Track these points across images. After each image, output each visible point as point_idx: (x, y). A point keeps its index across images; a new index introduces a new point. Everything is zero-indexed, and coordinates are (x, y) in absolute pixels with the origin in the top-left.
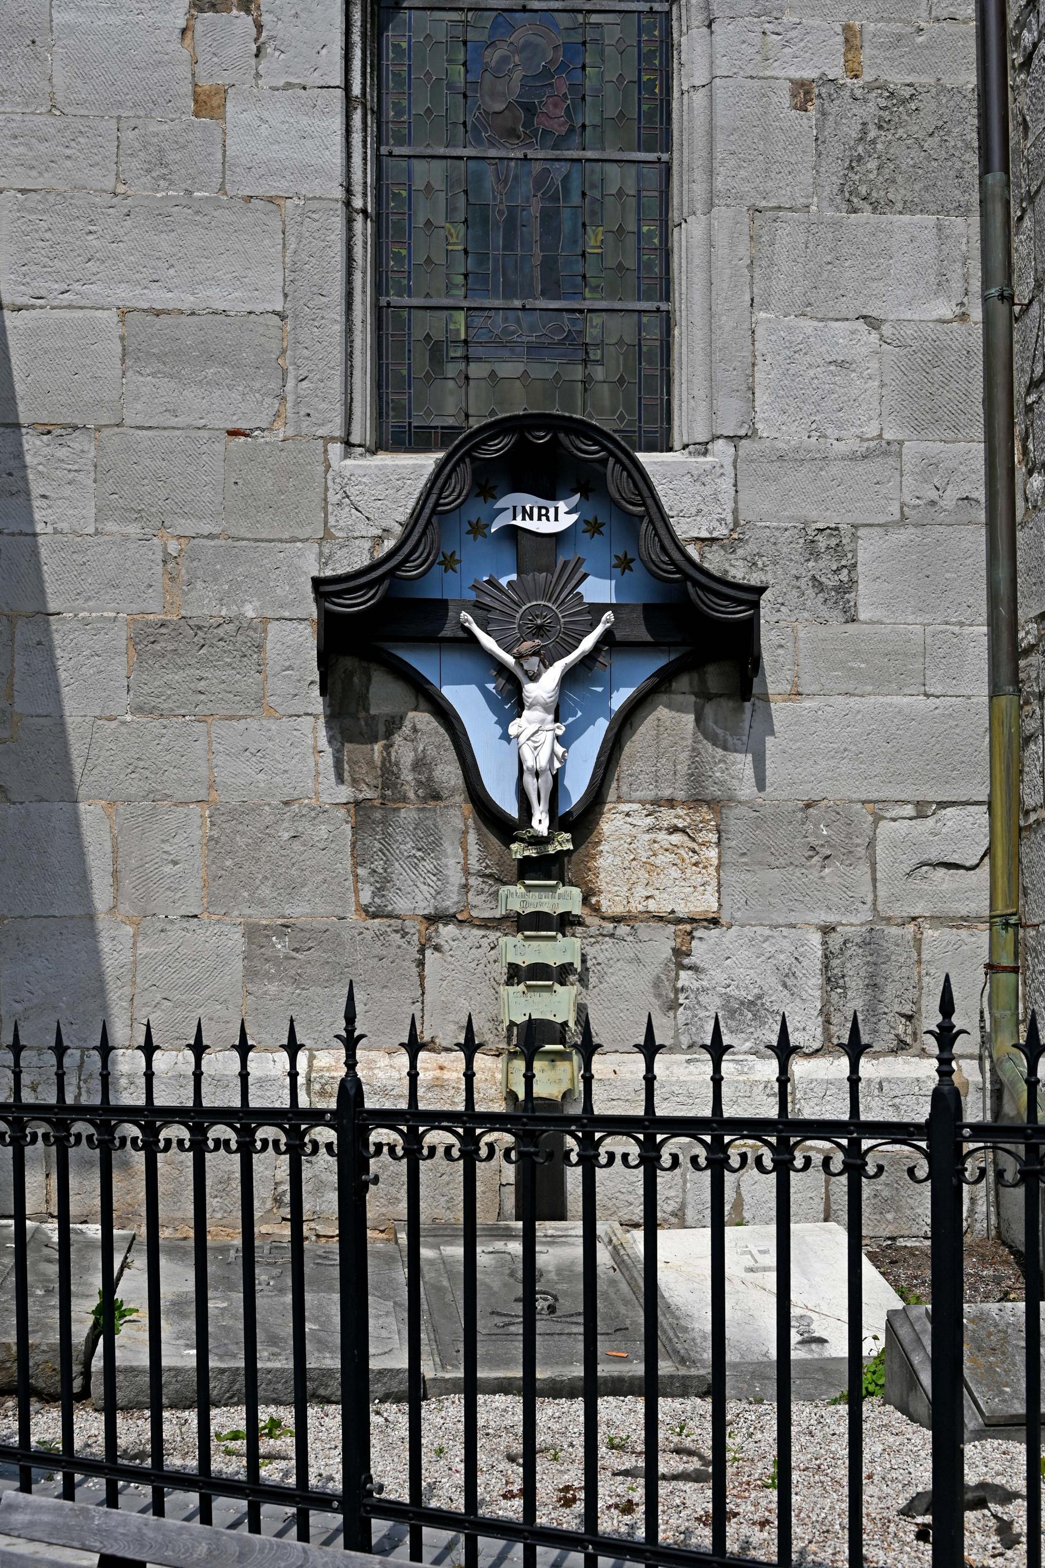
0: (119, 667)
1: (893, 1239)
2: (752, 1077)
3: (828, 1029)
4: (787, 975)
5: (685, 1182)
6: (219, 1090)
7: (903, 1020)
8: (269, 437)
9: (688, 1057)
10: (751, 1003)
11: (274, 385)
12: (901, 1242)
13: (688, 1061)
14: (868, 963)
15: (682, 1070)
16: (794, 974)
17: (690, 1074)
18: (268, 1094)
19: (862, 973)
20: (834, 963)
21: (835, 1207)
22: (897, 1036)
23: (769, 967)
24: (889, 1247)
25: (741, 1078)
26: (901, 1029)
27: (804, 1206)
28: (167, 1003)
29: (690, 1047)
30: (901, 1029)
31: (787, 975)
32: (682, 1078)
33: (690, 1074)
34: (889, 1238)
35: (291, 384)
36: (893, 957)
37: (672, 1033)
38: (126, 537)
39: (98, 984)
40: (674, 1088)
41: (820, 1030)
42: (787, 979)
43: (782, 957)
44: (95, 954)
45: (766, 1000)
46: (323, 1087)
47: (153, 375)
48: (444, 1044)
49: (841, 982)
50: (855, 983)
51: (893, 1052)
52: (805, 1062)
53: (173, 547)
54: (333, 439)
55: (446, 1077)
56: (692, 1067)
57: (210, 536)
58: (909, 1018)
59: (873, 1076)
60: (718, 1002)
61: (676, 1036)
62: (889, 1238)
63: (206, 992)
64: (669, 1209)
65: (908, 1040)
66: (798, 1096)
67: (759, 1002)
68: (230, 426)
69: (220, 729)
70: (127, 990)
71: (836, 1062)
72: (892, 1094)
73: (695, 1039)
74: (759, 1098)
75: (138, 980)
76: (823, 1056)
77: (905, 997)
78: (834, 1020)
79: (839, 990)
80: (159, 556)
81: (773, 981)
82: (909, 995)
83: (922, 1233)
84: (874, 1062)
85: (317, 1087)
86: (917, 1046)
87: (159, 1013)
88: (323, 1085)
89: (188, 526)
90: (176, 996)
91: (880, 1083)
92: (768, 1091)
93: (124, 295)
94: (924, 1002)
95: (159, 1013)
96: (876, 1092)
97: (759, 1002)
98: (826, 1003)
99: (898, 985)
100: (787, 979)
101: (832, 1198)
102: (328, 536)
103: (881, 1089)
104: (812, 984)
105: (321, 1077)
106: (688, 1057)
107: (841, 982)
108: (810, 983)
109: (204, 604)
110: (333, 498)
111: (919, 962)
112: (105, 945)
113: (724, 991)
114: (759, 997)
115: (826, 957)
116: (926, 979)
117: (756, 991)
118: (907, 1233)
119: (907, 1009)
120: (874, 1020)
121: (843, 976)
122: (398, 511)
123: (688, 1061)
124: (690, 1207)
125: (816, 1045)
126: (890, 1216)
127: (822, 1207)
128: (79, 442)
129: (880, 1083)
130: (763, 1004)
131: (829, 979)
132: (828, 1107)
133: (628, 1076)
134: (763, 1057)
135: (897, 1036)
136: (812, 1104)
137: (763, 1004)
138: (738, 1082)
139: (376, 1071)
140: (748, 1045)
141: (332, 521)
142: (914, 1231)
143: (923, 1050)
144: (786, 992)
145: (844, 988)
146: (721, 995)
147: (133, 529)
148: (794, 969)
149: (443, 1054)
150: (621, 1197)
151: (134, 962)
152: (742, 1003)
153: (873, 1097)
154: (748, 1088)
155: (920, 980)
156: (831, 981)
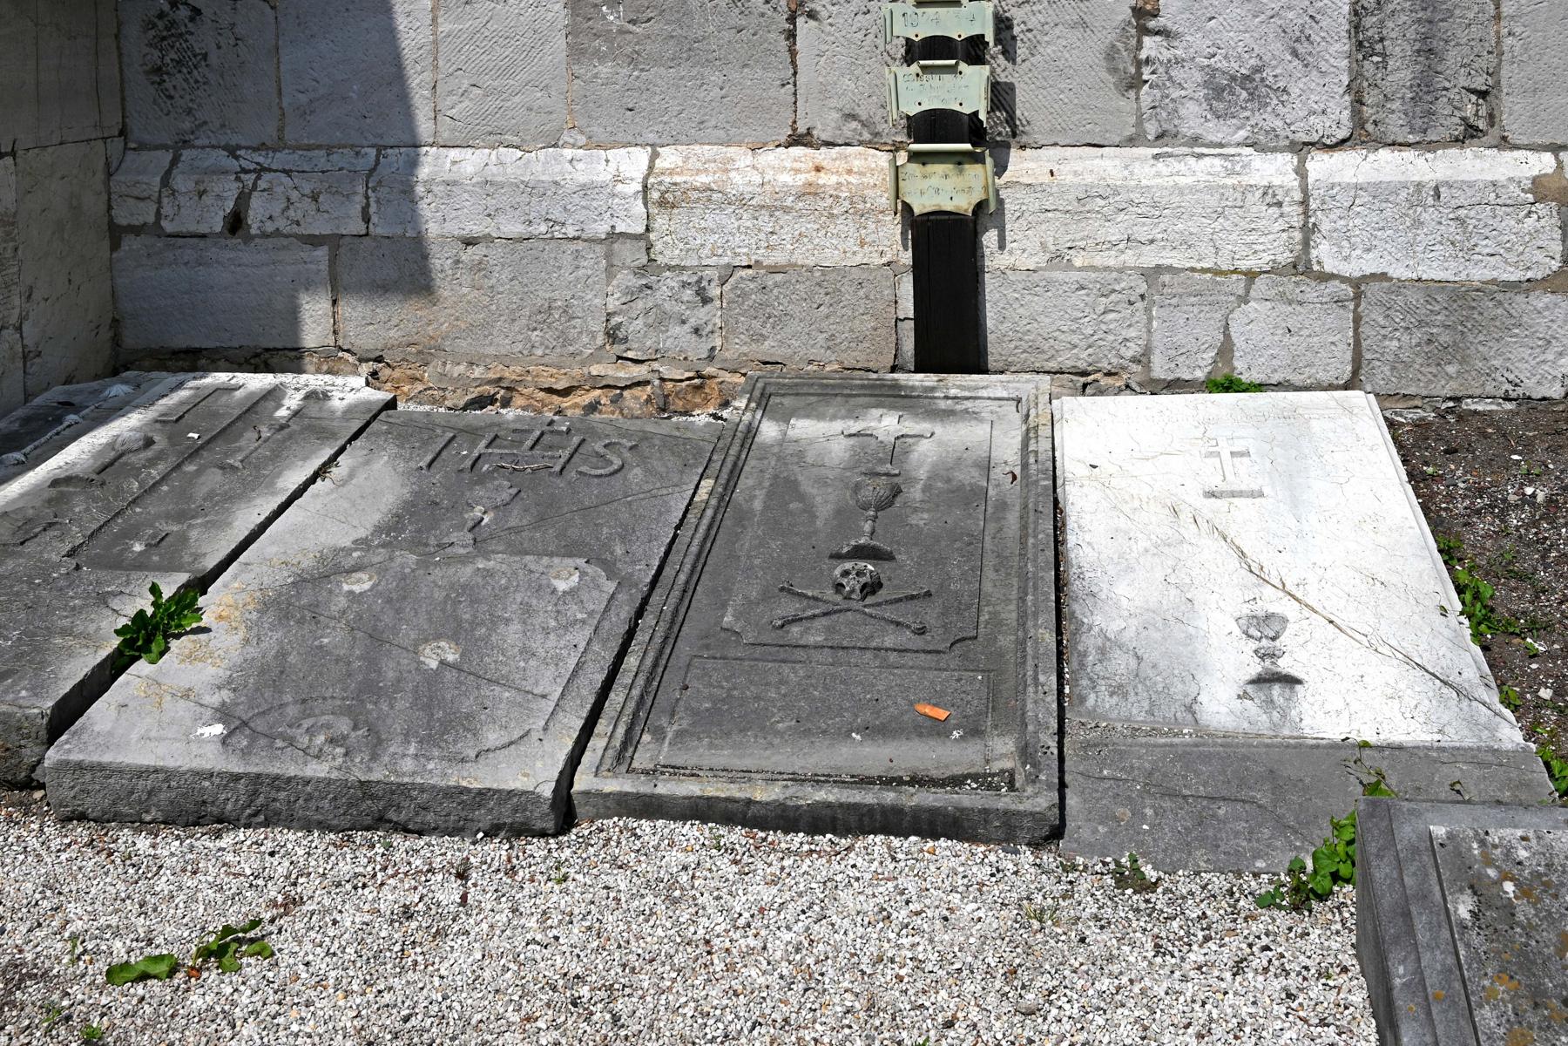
1: (1457, 399)
2: (1247, 180)
3: (1360, 112)
4: (1298, 40)
5: (1150, 320)
6: (535, 199)
7: (1474, 98)
9: (1156, 151)
10: (1246, 77)
12: (1469, 405)
13: (1156, 157)
14: (1419, 20)
15: (1147, 169)
16: (1308, 38)
17: (1158, 175)
18: (595, 204)
19: (1411, 34)
20: (1369, 21)
21: (1368, 356)
22: (1463, 119)
23: (1271, 29)
24: (1449, 411)
25: (1229, 181)
26: (1469, 110)
27: (1323, 354)
28: (476, 91)
29: (1158, 137)
30: (1469, 110)
31: (1298, 40)
32: (1144, 182)
33: (1158, 175)
34: (1450, 399)
36: (1457, 12)
37: (1133, 120)
39: (394, 70)
40: (1135, 196)
41: (1346, 114)
42: (1298, 45)
43: (1291, 15)
44: (390, 33)
45: (1268, 74)
46: (662, 196)
48: (824, 137)
49: (1378, 47)
50: (1400, 49)
51: (1458, 141)
52: (1326, 156)
55: (821, 182)
56: (1160, 165)
58: (1483, 94)
59: (1426, 179)
60: (1198, 77)
61: (1140, 122)
62: (1450, 399)
63: (523, 76)
64: (1129, 354)
65: (1481, 124)
66: (1313, 206)
67: (1257, 77)
70: (428, 76)
71: (1372, 157)
72: (1454, 203)
73: (1165, 126)
74: (1255, 209)
75: (441, 63)
76: (1353, 147)
77: (1476, 65)
78: (1369, 100)
79: (1376, 59)
81: (1278, 47)
82: (1481, 63)
83: (1501, 393)
84: (1429, 156)
85: (655, 195)
86: (1495, 132)
87: (467, 103)
88: (663, 194)
90: (486, 81)
91: (1436, 189)
92: (1268, 199)
94: (1504, 73)
95: (467, 103)
96: (1430, 201)
97: (1257, 77)
98: (1356, 76)
99: (1466, 50)
100: (1298, 45)
101: (1364, 344)
103: (1437, 195)
104: (1335, 52)
105: (660, 183)
106: (1156, 151)
107: (1378, 47)
108: (1332, 50)
111: (1498, 17)
112: (402, 23)
113: (1206, 62)
114: (1258, 70)
115: (1356, 13)
116: (1509, 41)
117: (1253, 62)
118: (1478, 392)
119: (1479, 83)
120: (1429, 98)
121: (1382, 40)
123: (1156, 157)
124: (1157, 352)
125: (1342, 134)
126: (1451, 369)
127: (1349, 355)
129: (1436, 189)
130: (1263, 80)
131: (1360, 44)
132: (1358, 221)
133: (1070, 179)
134: (1263, 151)
135: (1463, 119)
136: (1332, 216)
137: (1263, 80)
138: (1225, 186)
139: (733, 174)
140: (1242, 134)
142: (1489, 389)
143: (1504, 138)
144: (1296, 62)
145: (1384, 55)
146: (1202, 68)
148: (1308, 32)
149: (823, 149)
150: (1062, 337)
151: (435, 42)
152: (1233, 78)
153: (1425, 207)
154: (1238, 195)
155: (1498, 43)
156: (1364, 46)
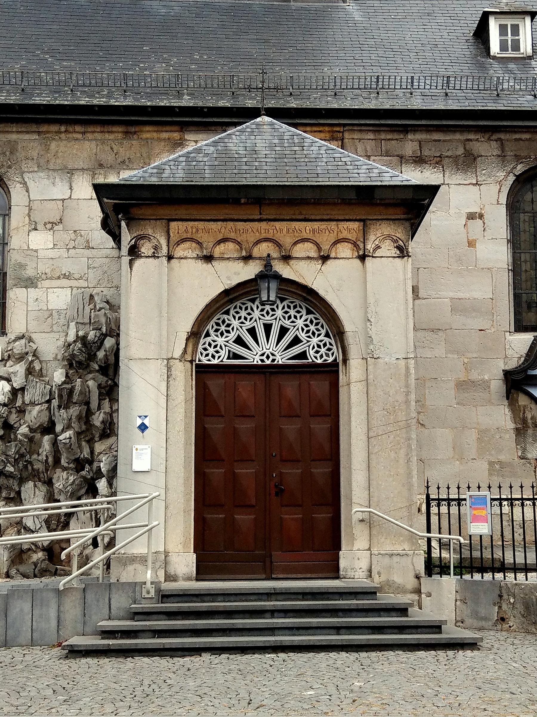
0: (453, 392)
8: (489, 331)
11: (491, 317)
35: (495, 317)
38: (453, 358)
47: (459, 315)
53: (466, 361)
54: (507, 332)
57: (476, 358)
68: (480, 329)
69: (479, 408)
80: (462, 363)
89: (470, 355)
93: (451, 294)
102: (506, 357)
109: (474, 376)
110: (507, 347)
122: (524, 349)
128: (440, 333)
141: (507, 353)
147: (456, 356)
